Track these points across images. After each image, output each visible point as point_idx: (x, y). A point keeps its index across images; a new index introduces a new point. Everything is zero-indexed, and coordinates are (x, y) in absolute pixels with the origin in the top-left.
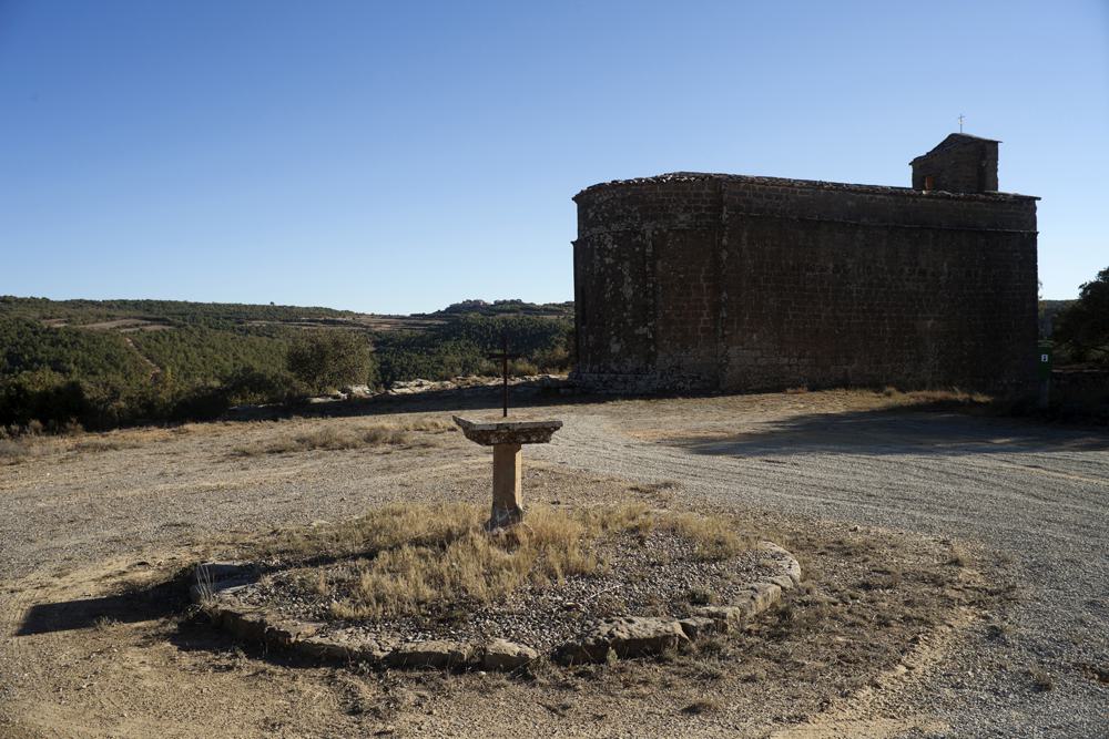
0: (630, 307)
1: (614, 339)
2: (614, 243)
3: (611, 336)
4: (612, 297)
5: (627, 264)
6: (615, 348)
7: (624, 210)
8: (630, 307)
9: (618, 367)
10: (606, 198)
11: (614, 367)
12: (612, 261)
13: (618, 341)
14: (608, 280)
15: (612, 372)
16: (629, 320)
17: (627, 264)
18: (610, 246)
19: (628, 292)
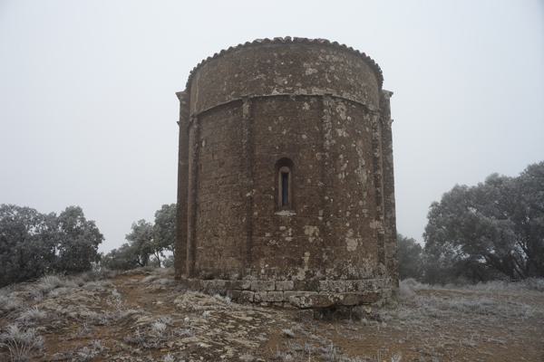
0: (365, 194)
1: (351, 233)
2: (347, 115)
3: (345, 232)
4: (346, 177)
5: (360, 143)
6: (352, 245)
7: (355, 81)
8: (365, 194)
9: (357, 270)
10: (335, 59)
11: (352, 271)
12: (345, 135)
13: (354, 236)
14: (341, 156)
15: (351, 277)
16: (365, 211)
17: (360, 143)
18: (342, 116)
19: (363, 176)
